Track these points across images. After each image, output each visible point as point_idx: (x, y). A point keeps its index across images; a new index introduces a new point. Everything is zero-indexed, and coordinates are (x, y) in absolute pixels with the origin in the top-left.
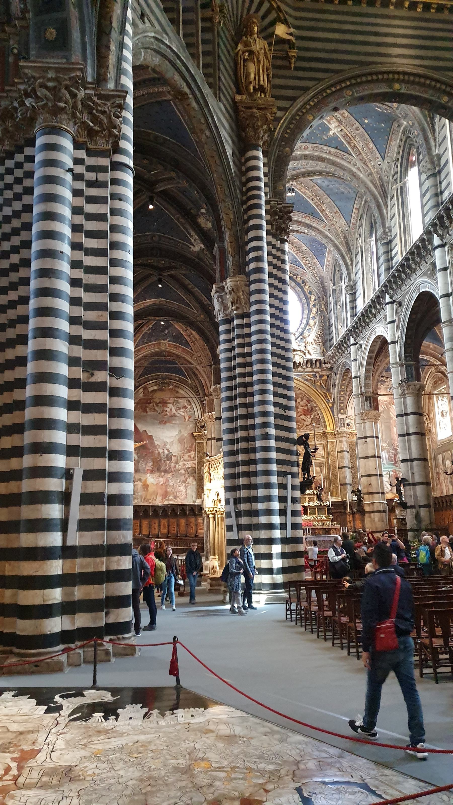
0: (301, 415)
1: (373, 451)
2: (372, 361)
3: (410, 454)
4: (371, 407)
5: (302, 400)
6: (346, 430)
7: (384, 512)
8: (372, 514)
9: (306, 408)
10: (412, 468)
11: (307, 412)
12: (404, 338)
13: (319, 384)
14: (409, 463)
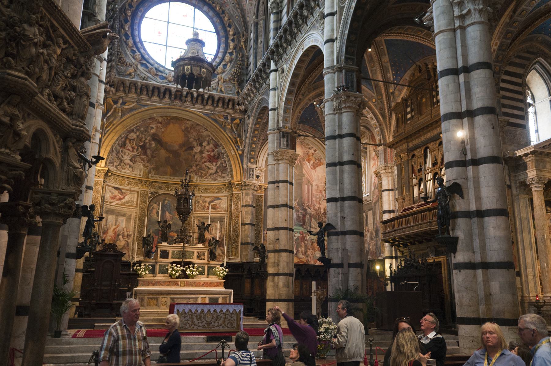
0: (205, 162)
1: (285, 199)
2: (295, 89)
3: (341, 190)
4: (287, 145)
5: (209, 144)
6: (254, 181)
7: (291, 275)
8: (276, 278)
9: (212, 154)
10: (342, 210)
11: (213, 159)
12: (347, 32)
13: (229, 127)
14: (339, 203)
